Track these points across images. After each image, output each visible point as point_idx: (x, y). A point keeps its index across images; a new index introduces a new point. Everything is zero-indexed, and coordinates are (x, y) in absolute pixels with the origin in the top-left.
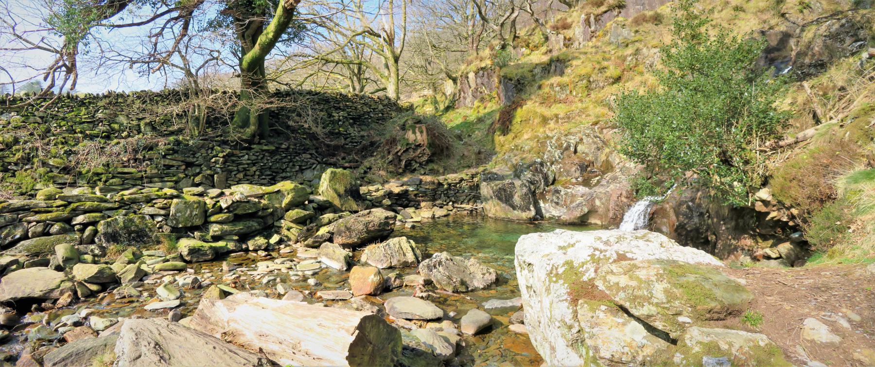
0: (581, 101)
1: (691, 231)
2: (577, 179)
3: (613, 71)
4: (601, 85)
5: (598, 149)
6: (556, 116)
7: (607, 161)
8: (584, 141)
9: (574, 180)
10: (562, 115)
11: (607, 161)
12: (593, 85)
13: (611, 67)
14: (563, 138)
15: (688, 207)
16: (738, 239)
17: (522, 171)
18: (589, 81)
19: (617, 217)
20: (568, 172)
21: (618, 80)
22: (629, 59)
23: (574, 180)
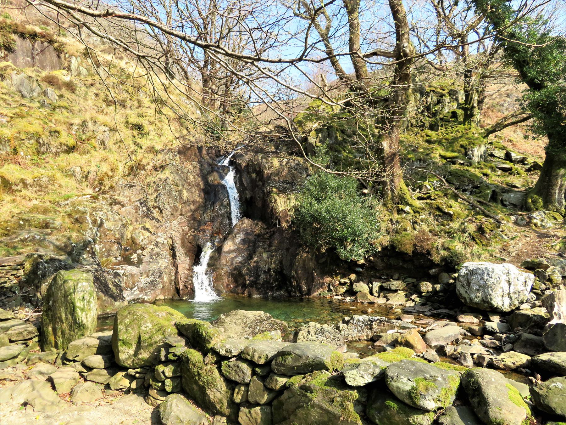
0: (38, 165)
1: (263, 284)
2: (116, 258)
3: (67, 139)
4: (54, 150)
5: (124, 226)
6: (23, 181)
7: (132, 238)
8: (109, 217)
9: (114, 260)
10: (29, 181)
11: (132, 238)
12: (44, 149)
13: (64, 134)
14: (94, 213)
15: (248, 269)
16: (323, 279)
17: (80, 254)
18: (40, 143)
19: (187, 288)
20: (109, 251)
21: (71, 149)
22: (75, 127)
23: (114, 260)
